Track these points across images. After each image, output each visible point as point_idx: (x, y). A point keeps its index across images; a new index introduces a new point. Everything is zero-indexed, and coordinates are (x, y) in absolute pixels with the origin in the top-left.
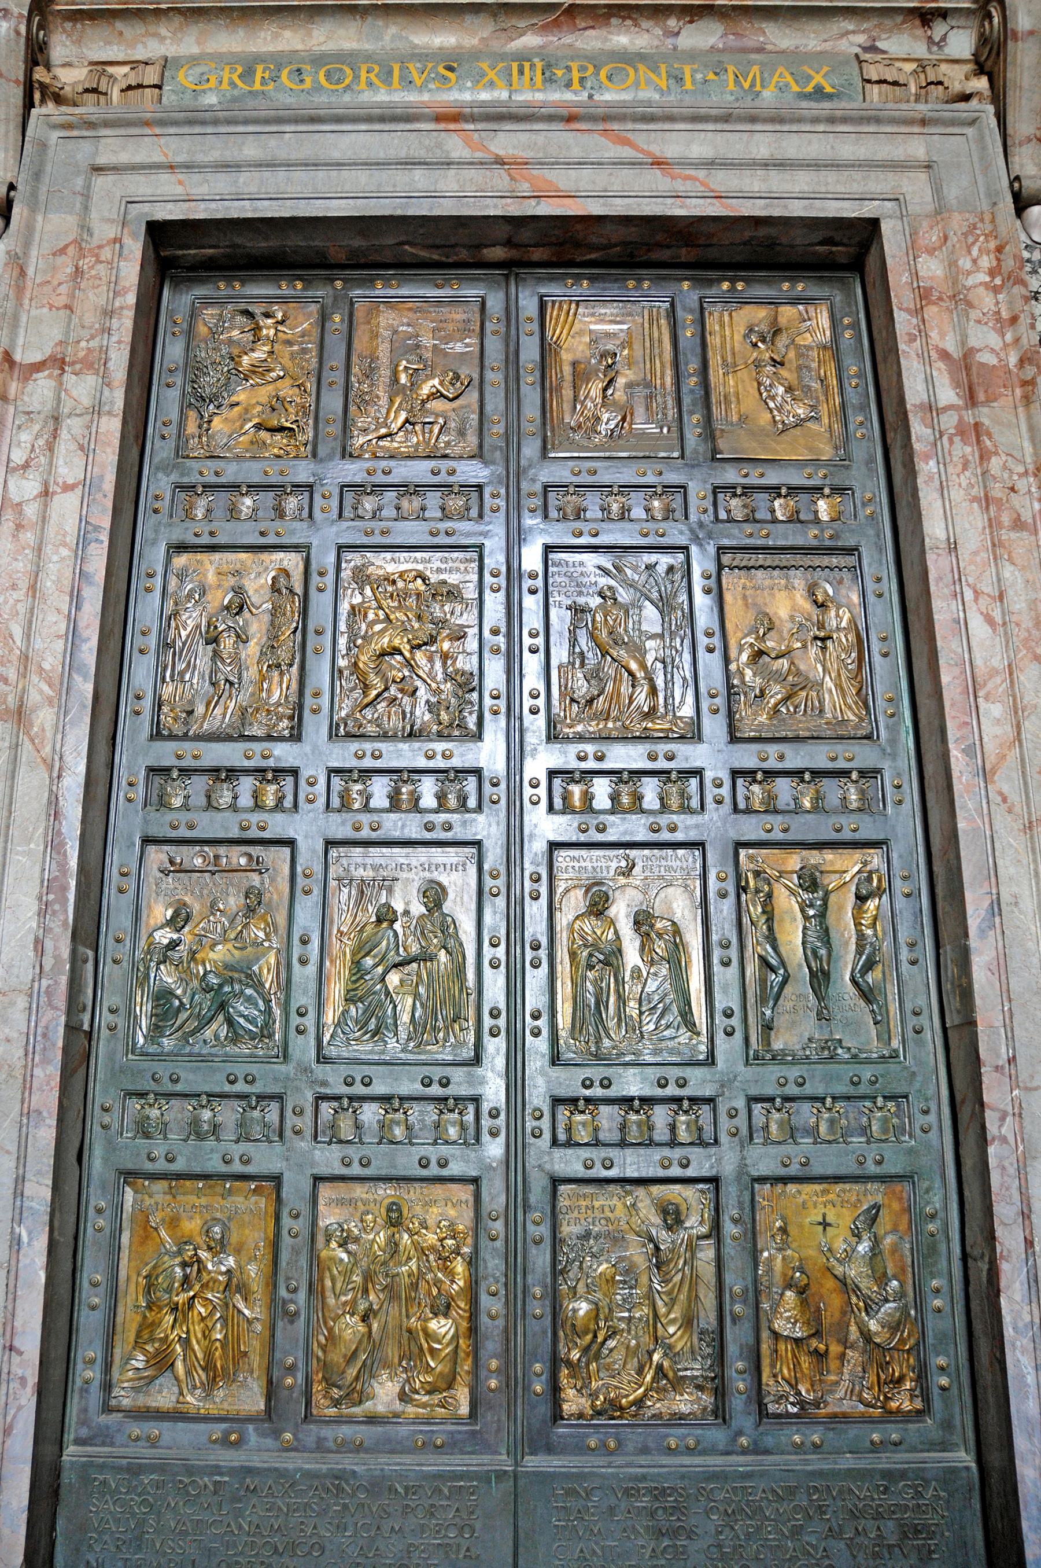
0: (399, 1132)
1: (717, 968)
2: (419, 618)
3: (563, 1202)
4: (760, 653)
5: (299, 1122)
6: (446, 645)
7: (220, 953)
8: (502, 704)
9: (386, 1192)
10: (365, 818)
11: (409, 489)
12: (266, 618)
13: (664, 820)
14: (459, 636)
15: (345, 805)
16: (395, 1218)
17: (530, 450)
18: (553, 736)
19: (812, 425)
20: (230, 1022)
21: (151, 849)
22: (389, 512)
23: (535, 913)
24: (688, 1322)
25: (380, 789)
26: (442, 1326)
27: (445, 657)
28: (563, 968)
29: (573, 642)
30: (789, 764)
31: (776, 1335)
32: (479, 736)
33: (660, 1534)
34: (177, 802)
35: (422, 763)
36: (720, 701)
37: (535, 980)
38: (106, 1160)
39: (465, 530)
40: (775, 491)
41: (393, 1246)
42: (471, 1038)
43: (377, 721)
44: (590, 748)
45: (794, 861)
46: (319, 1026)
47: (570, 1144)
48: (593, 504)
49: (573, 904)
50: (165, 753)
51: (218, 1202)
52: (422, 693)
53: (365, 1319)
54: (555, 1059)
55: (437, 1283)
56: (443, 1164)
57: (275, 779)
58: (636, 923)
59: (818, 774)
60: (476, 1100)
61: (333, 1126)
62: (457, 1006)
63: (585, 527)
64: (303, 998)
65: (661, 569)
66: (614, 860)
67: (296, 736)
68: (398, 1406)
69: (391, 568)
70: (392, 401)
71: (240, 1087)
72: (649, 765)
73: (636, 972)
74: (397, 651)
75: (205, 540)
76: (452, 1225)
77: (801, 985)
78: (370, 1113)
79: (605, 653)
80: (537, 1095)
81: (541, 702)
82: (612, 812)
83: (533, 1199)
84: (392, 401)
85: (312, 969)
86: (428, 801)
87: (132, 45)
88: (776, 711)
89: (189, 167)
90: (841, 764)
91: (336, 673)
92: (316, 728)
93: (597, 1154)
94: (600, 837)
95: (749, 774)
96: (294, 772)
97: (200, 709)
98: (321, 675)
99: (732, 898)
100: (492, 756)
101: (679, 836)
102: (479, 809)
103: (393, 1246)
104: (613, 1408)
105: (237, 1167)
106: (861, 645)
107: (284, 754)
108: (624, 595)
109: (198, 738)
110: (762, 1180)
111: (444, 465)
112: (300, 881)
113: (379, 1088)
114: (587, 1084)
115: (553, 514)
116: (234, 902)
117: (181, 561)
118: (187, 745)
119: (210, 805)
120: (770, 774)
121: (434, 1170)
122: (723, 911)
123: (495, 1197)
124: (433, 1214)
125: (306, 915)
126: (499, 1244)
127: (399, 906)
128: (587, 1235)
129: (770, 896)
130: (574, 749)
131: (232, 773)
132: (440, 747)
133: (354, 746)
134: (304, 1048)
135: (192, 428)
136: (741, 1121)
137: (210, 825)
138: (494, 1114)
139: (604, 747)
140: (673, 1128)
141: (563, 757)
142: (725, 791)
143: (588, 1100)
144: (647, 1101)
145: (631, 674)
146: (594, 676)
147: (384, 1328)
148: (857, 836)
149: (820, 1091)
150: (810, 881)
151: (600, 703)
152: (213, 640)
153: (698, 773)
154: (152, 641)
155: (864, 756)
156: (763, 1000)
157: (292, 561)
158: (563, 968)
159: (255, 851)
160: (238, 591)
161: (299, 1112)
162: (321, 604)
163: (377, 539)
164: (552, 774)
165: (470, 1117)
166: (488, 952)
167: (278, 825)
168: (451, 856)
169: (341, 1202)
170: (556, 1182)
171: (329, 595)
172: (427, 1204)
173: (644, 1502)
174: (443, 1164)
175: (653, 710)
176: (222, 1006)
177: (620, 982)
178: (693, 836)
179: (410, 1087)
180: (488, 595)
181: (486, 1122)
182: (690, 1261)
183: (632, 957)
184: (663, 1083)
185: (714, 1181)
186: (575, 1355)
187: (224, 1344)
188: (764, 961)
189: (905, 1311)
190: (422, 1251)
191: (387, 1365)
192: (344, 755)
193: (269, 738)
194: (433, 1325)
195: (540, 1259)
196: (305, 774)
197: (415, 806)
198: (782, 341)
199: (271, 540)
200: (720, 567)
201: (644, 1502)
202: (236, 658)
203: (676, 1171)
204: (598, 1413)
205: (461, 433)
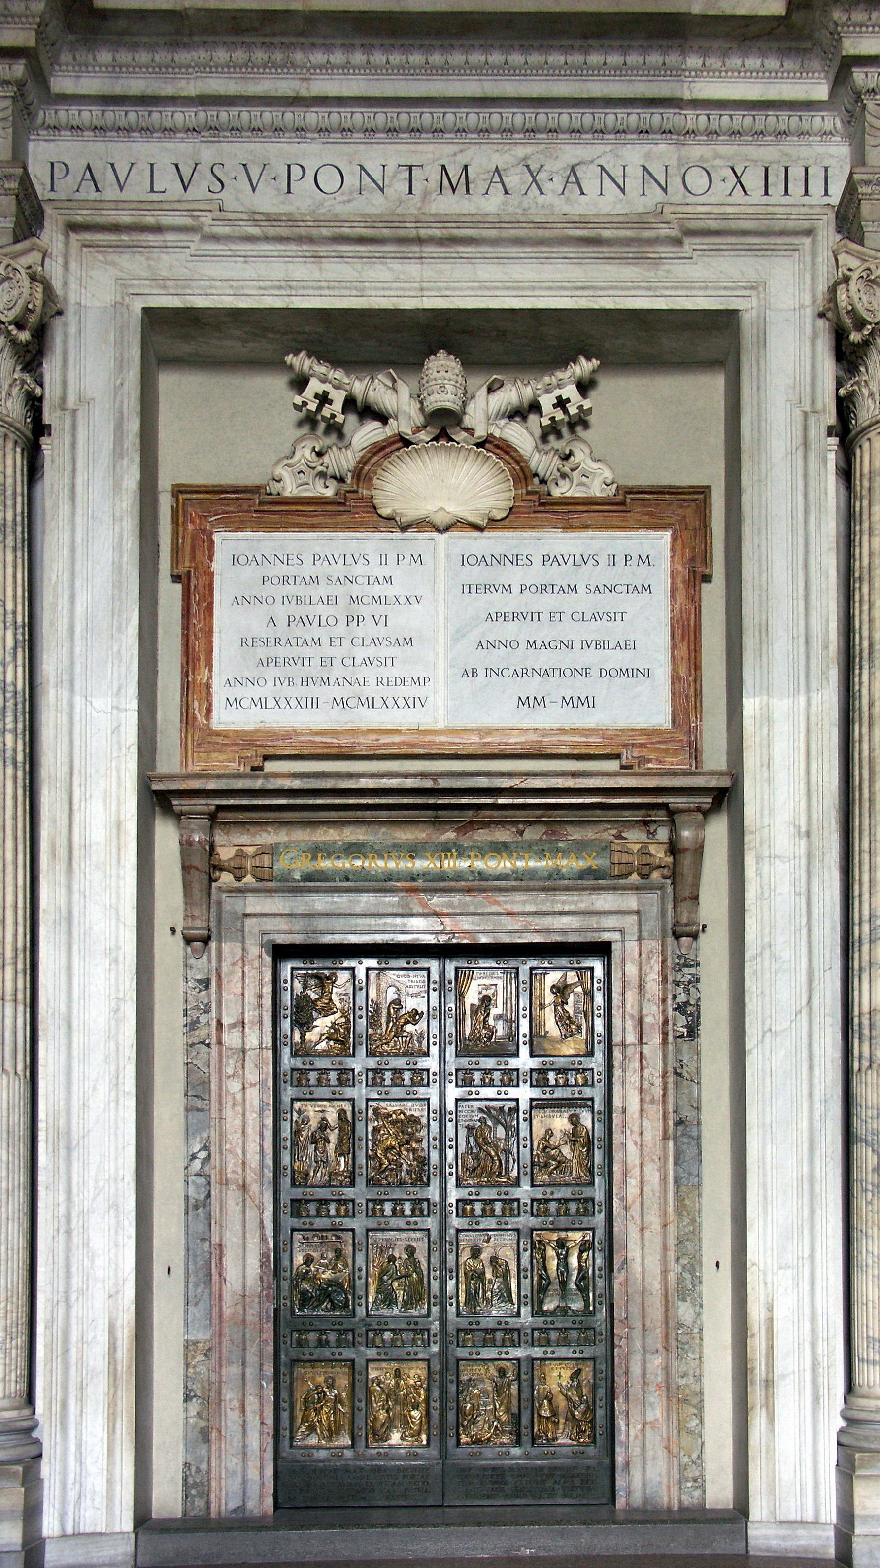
0: (399, 1343)
1: (522, 1280)
2: (402, 1132)
3: (461, 1368)
4: (546, 1147)
5: (360, 1340)
6: (414, 1145)
7: (327, 1275)
8: (438, 1170)
9: (395, 1365)
10: (382, 1220)
11: (398, 1071)
12: (337, 1131)
13: (504, 1220)
14: (419, 1141)
15: (374, 1215)
16: (398, 1374)
17: (450, 1050)
18: (458, 1185)
19: (578, 1037)
20: (332, 1302)
21: (295, 1233)
22: (388, 1082)
23: (451, 1258)
24: (508, 1411)
25: (388, 1207)
26: (415, 1414)
27: (414, 1150)
28: (462, 1279)
29: (468, 1143)
30: (555, 1196)
31: (540, 1416)
32: (428, 1185)
33: (496, 1483)
34: (304, 1214)
35: (405, 1197)
36: (528, 1169)
37: (451, 1285)
38: (286, 1355)
39: (422, 1091)
40: (558, 1071)
41: (397, 1384)
42: (426, 1306)
43: (386, 1178)
44: (473, 1190)
45: (555, 1236)
46: (367, 1302)
47: (463, 1346)
48: (477, 1076)
49: (465, 1256)
50: (298, 1193)
51: (330, 1370)
52: (405, 1167)
53: (387, 1411)
54: (458, 1314)
55: (414, 1398)
56: (416, 1354)
57: (345, 1204)
58: (491, 1261)
59: (567, 1200)
60: (428, 1330)
61: (373, 1340)
62: (420, 1295)
63: (473, 1089)
64: (361, 1292)
65: (506, 1109)
66: (483, 1236)
67: (353, 1184)
68: (400, 1442)
69: (390, 1109)
70: (388, 1026)
71: (337, 1327)
72: (497, 1197)
73: (490, 1282)
74: (393, 1148)
75: (308, 1096)
76: (419, 1377)
77: (556, 1286)
78: (387, 1335)
79: (481, 1148)
80: (451, 1329)
81: (454, 1170)
82: (482, 1217)
83: (450, 1367)
84: (388, 1026)
85: (363, 1281)
86: (408, 1212)
87: (254, 835)
88: (551, 1172)
89: (290, 915)
90: (577, 1196)
91: (368, 1157)
92: (361, 1182)
93: (474, 1350)
94: (477, 1227)
95: (539, 1201)
96: (353, 1201)
97: (312, 1173)
98: (361, 1160)
99: (529, 1252)
100: (433, 1195)
101: (509, 1227)
102: (428, 1216)
103: (397, 1384)
104: (478, 1441)
105: (337, 1357)
106: (589, 1144)
107: (349, 1193)
108: (489, 1123)
109: (312, 1186)
110: (537, 1359)
111: (413, 1059)
112: (357, 1246)
113: (392, 1327)
114: (470, 1324)
115: (460, 1083)
116: (331, 1255)
117: (297, 1105)
118: (308, 1190)
119: (318, 1215)
120: (547, 1201)
121: (413, 1356)
122: (526, 1257)
123: (436, 1366)
124: (412, 1373)
125: (360, 1260)
126: (437, 1383)
127: (397, 1255)
128: (470, 1379)
129: (545, 1250)
130: (467, 1190)
131: (327, 1201)
132: (412, 1189)
133: (376, 1190)
134: (361, 1311)
135: (297, 1037)
136: (529, 1338)
137: (320, 1223)
138: (435, 1335)
139: (479, 1189)
140: (503, 1340)
141: (463, 1193)
142: (528, 1208)
143: (471, 1330)
144: (494, 1331)
145: (492, 1158)
146: (477, 1158)
147: (394, 1414)
148: (583, 1226)
149: (560, 1326)
150: (561, 1244)
151: (478, 1171)
152: (314, 1141)
153: (518, 1200)
154: (288, 1144)
155: (587, 1192)
156: (539, 1292)
157: (347, 1106)
158: (462, 1279)
159: (339, 1233)
160: (324, 1119)
161: (360, 1335)
162: (360, 1126)
163: (384, 1096)
164: (458, 1201)
165: (426, 1337)
166: (432, 1273)
167: (348, 1223)
168: (418, 1235)
169: (377, 1369)
170: (458, 1360)
171: (364, 1122)
172: (410, 1369)
173: (490, 1472)
174: (416, 1354)
175: (500, 1173)
176: (329, 1296)
177: (484, 1285)
178: (515, 1226)
179: (403, 1326)
180: (431, 1122)
181: (432, 1339)
182: (509, 1389)
183: (489, 1275)
184: (500, 1323)
185: (518, 1360)
186: (465, 1423)
187: (335, 1420)
188: (541, 1277)
189: (588, 1407)
190: (407, 1386)
191: (396, 1427)
192: (373, 1193)
193: (341, 1186)
194: (413, 1413)
195: (452, 1388)
196: (357, 1201)
197: (402, 1214)
198: (569, 990)
199: (337, 1096)
200: (531, 1108)
201: (490, 1472)
202: (325, 1152)
203: (503, 1356)
204: (473, 1443)
205: (420, 1043)
